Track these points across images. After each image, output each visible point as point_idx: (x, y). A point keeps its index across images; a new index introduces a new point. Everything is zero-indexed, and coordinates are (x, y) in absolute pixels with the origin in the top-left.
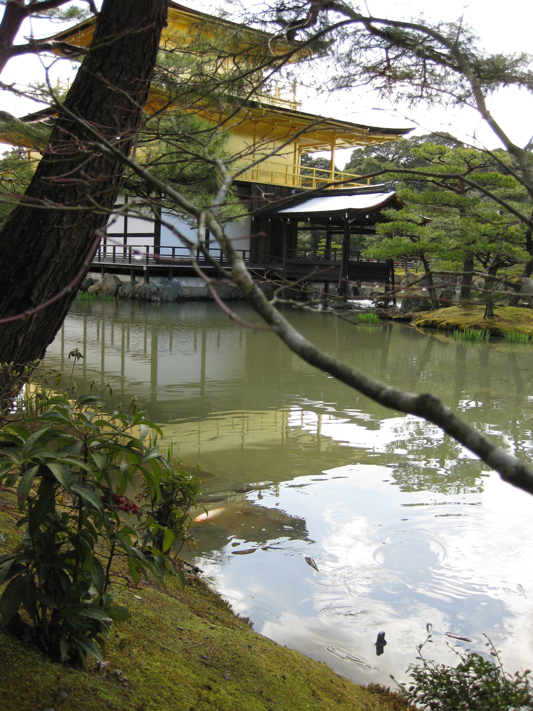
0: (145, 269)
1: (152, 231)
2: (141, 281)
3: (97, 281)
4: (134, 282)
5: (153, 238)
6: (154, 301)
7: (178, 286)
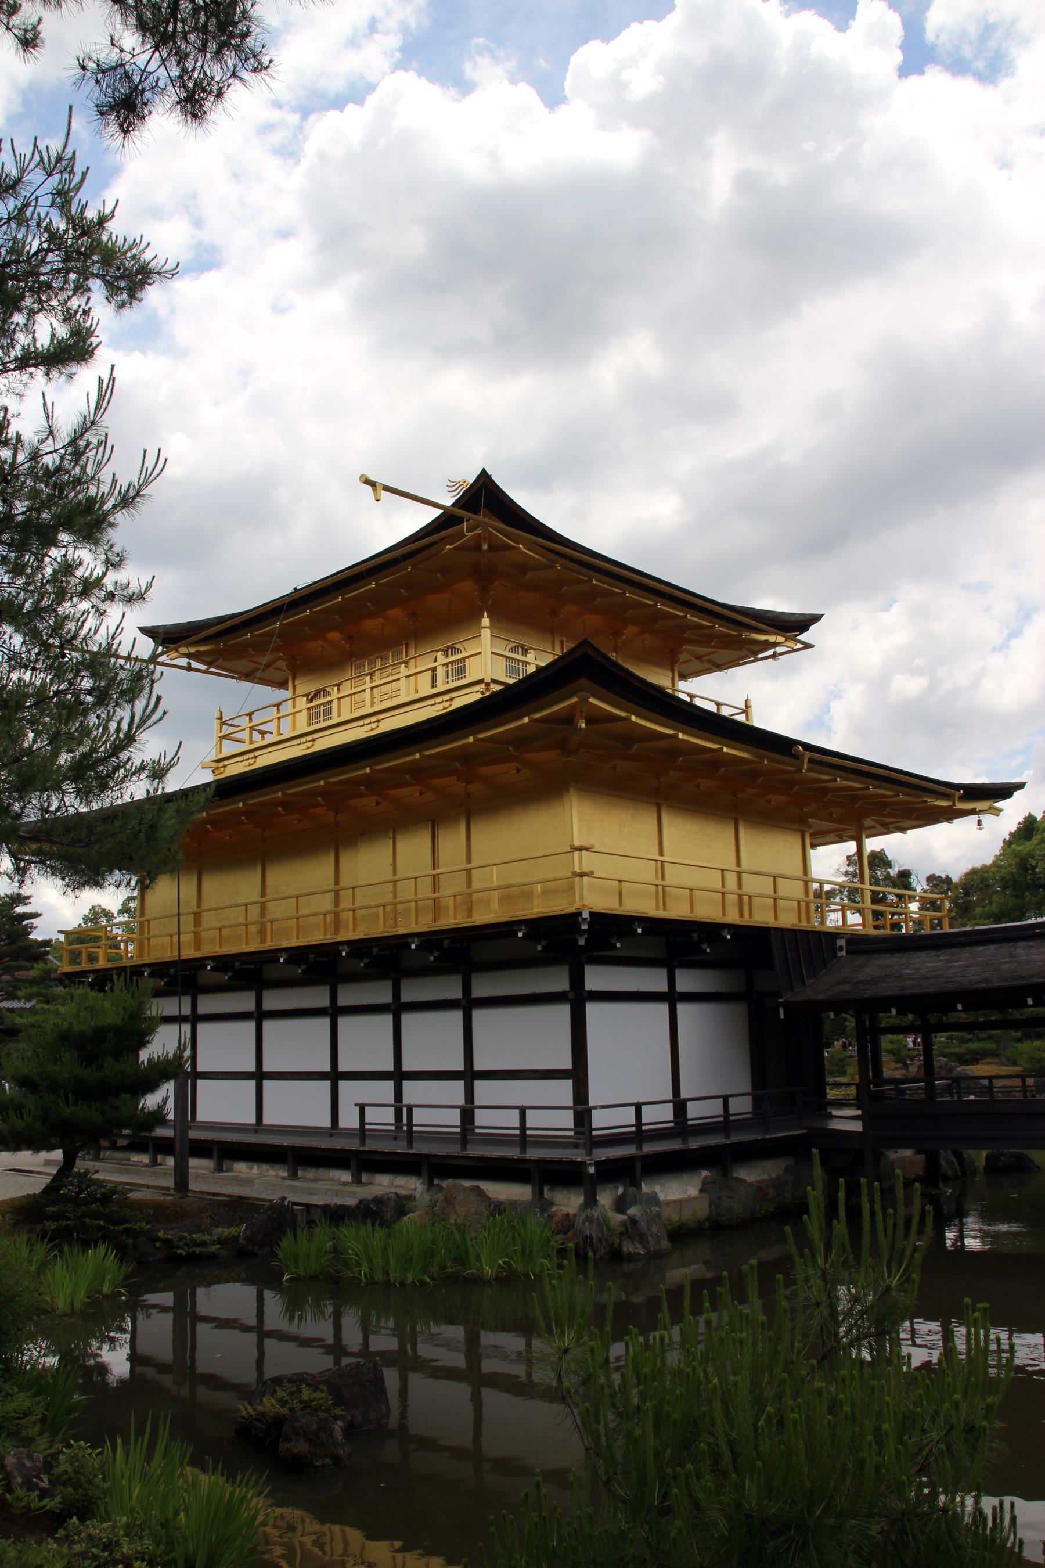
0: (592, 1170)
1: (567, 1064)
2: (569, 1202)
3: (410, 1198)
4: (545, 1206)
5: (567, 1085)
6: (631, 1258)
7: (653, 1199)
